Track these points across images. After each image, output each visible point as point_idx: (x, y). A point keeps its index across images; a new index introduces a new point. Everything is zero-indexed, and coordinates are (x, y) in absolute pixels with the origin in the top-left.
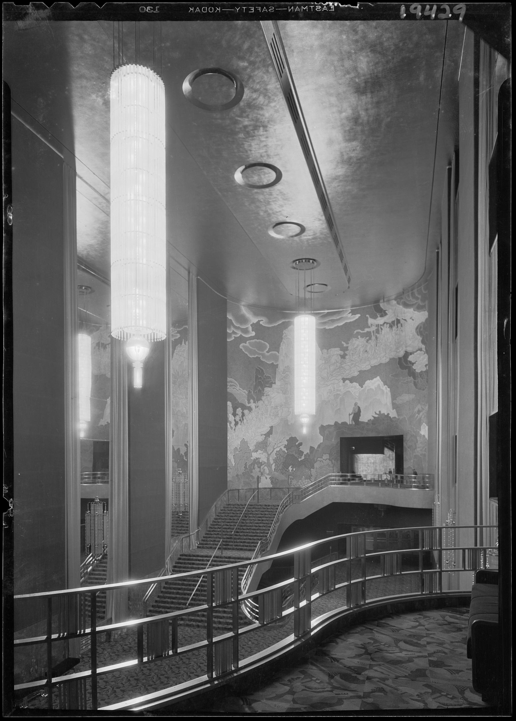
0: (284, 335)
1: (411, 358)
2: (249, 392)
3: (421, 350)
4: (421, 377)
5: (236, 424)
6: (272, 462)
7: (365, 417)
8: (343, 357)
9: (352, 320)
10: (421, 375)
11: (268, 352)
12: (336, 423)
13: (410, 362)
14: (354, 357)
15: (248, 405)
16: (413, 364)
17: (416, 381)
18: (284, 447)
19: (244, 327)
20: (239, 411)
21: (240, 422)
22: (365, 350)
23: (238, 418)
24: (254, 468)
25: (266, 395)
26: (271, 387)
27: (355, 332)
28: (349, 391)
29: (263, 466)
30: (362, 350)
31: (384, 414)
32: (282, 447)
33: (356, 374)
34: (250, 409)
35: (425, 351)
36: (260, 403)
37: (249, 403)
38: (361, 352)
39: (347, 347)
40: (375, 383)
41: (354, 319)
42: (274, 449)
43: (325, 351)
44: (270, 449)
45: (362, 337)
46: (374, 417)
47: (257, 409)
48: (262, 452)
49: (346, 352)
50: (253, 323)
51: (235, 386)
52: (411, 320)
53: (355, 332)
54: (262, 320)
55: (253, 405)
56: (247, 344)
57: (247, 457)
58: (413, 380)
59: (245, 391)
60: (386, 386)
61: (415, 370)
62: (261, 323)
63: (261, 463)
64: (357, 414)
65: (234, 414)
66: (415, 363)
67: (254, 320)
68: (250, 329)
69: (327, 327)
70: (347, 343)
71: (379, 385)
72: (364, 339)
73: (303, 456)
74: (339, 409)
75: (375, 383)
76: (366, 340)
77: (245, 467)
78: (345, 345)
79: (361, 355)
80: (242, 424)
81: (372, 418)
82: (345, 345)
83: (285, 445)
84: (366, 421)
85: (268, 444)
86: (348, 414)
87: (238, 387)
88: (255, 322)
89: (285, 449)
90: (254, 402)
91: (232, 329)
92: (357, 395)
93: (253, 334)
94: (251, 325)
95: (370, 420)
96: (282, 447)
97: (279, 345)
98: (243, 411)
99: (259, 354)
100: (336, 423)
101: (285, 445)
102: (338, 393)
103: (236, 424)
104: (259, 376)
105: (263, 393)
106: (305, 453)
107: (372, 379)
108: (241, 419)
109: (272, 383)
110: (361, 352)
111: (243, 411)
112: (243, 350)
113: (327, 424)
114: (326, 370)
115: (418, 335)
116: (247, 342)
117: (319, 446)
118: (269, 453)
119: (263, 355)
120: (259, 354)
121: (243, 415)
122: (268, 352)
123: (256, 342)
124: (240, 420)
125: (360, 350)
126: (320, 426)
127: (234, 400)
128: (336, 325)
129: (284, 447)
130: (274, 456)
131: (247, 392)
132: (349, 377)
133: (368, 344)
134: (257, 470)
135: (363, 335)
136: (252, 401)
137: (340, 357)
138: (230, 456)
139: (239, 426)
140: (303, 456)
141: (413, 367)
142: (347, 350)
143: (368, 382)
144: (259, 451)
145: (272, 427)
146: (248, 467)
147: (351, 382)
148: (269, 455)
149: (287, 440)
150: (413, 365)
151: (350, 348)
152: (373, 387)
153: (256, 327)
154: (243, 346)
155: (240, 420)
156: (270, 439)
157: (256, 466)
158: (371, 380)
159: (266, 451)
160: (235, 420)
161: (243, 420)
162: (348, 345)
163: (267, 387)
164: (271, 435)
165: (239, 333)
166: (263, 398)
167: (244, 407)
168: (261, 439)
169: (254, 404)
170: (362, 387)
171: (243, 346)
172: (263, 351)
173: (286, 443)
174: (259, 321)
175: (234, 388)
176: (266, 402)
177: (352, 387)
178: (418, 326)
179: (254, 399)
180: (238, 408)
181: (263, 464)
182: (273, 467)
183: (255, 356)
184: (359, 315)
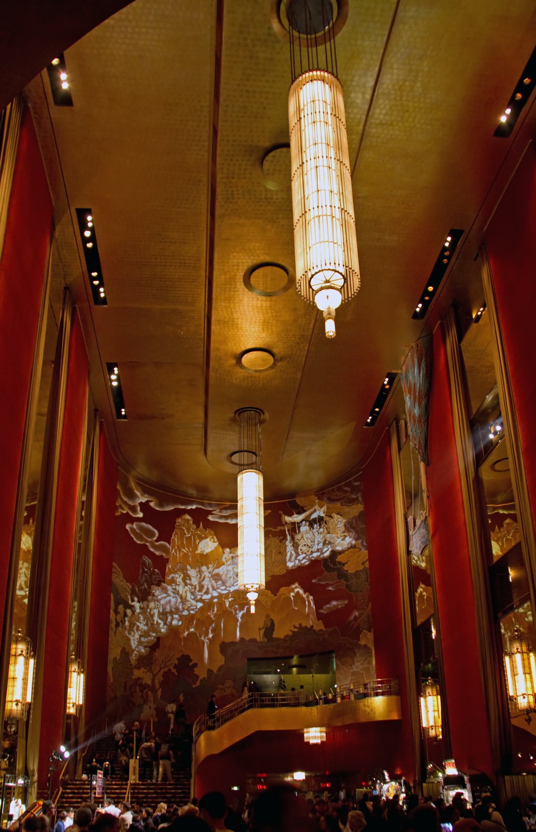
1: (339, 558)
2: (133, 587)
4: (356, 577)
6: (157, 686)
10: (356, 575)
13: (340, 563)
15: (133, 604)
16: (344, 564)
17: (350, 583)
18: (174, 667)
20: (121, 608)
21: (121, 624)
22: (278, 552)
23: (119, 619)
29: (146, 690)
30: (274, 551)
32: (171, 668)
37: (133, 601)
38: (274, 554)
42: (161, 668)
48: (145, 670)
58: (345, 582)
59: (129, 584)
60: (307, 593)
61: (347, 571)
63: (144, 685)
64: (269, 629)
66: (347, 563)
72: (276, 538)
73: (199, 681)
76: (279, 539)
77: (125, 688)
79: (273, 557)
80: (124, 627)
83: (175, 665)
85: (153, 661)
86: (258, 628)
87: (121, 578)
89: (174, 671)
90: (139, 602)
96: (171, 668)
101: (175, 665)
104: (146, 570)
105: (149, 592)
106: (201, 678)
108: (123, 620)
110: (274, 554)
113: (230, 641)
117: (219, 669)
118: (155, 673)
124: (122, 621)
125: (271, 551)
126: (220, 642)
129: (174, 667)
130: (160, 678)
131: (130, 587)
133: (282, 544)
139: (120, 628)
140: (199, 681)
141: (344, 568)
144: (142, 670)
146: (128, 688)
148: (154, 676)
149: (178, 659)
150: (344, 566)
155: (122, 621)
156: (157, 654)
157: (138, 688)
158: (287, 587)
159: (150, 670)
164: (157, 650)
169: (139, 604)
173: (176, 662)
179: (138, 597)
180: (120, 604)
182: (159, 693)
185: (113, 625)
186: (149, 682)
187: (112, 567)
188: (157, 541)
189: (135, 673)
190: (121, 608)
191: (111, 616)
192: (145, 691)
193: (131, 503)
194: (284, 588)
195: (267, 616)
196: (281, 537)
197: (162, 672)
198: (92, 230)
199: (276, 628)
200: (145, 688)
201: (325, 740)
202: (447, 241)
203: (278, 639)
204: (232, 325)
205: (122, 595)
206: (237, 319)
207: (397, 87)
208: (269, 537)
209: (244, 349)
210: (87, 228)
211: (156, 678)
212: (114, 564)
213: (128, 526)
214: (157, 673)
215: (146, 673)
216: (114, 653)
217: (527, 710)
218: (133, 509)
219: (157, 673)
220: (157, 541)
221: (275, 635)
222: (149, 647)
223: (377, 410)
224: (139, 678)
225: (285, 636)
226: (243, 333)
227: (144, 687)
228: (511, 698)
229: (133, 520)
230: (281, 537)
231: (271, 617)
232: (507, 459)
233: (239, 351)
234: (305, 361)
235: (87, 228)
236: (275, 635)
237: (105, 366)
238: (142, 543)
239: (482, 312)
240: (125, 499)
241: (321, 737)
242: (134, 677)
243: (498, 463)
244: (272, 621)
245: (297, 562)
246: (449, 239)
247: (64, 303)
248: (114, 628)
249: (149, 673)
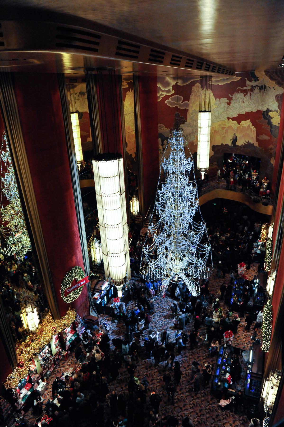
0: (192, 90)
7: (240, 143)
8: (229, 104)
9: (236, 81)
12: (222, 144)
14: (236, 105)
19: (167, 89)
26: (184, 123)
27: (237, 88)
28: (231, 126)
30: (241, 101)
31: (251, 143)
33: (236, 115)
39: (232, 98)
40: (247, 123)
41: (238, 80)
43: (218, 99)
45: (242, 92)
46: (245, 144)
49: (231, 101)
50: (173, 85)
51: (162, 128)
53: (237, 88)
54: (179, 82)
56: (170, 100)
62: (178, 84)
64: (235, 140)
67: (173, 83)
68: (172, 89)
69: (220, 84)
70: (232, 95)
71: (249, 125)
74: (225, 136)
75: (247, 123)
78: (231, 96)
81: (244, 144)
82: (231, 96)
84: (240, 145)
88: (174, 84)
91: (161, 92)
92: (236, 128)
93: (173, 92)
94: (172, 87)
95: (242, 145)
97: (189, 97)
99: (177, 104)
100: (222, 144)
102: (225, 126)
107: (246, 120)
112: (167, 104)
114: (218, 112)
116: (170, 98)
119: (180, 105)
120: (177, 104)
123: (175, 97)
128: (225, 83)
131: (170, 130)
132: (232, 117)
135: (242, 91)
137: (227, 104)
142: (232, 100)
143: (243, 122)
147: (233, 120)
151: (233, 99)
152: (246, 126)
153: (175, 87)
154: (167, 102)
162: (232, 97)
163: (181, 124)
165: (165, 94)
170: (239, 124)
171: (167, 102)
174: (177, 83)
177: (233, 124)
183: (174, 106)
184: (241, 77)
188: (182, 102)
194: (243, 121)
195: (234, 134)
196: (245, 94)
199: (237, 140)
203: (238, 146)
208: (239, 93)
220: (182, 102)
221: (237, 144)
225: (241, 145)
230: (245, 94)
231: (236, 135)
236: (237, 144)
244: (236, 137)
245: (251, 108)
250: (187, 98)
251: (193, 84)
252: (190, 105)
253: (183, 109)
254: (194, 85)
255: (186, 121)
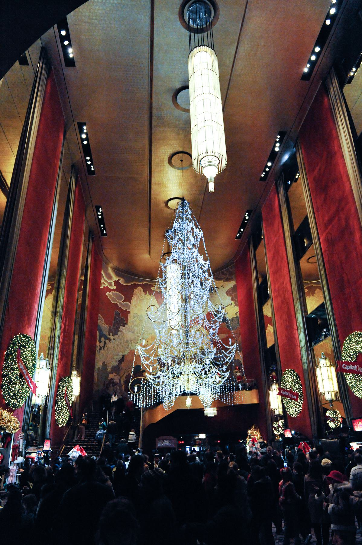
2: (110, 327)
3: (231, 304)
5: (100, 349)
6: (122, 383)
11: (123, 302)
15: (109, 337)
20: (103, 339)
21: (103, 348)
23: (102, 345)
24: (110, 387)
25: (121, 332)
26: (124, 326)
29: (116, 386)
34: (110, 340)
35: (234, 304)
36: (116, 337)
37: (109, 335)
42: (125, 373)
44: (121, 373)
47: (114, 340)
48: (116, 374)
52: (222, 287)
55: (111, 337)
57: (106, 377)
59: (107, 325)
63: (115, 383)
65: (100, 342)
77: (104, 385)
87: (103, 322)
90: (113, 335)
98: (105, 340)
103: (100, 349)
109: (125, 324)
111: (105, 340)
115: (228, 295)
119: (120, 303)
121: (105, 343)
122: (123, 302)
124: (103, 347)
127: (100, 331)
131: (108, 327)
134: (112, 388)
136: (111, 334)
138: (95, 374)
139: (102, 351)
144: (114, 374)
145: (123, 356)
148: (121, 377)
155: (103, 347)
156: (122, 365)
159: (118, 374)
160: (100, 346)
161: (105, 347)
163: (121, 326)
166: (119, 333)
167: (106, 338)
168: (115, 364)
172: (120, 300)
175: (101, 322)
176: (121, 337)
178: (228, 290)
181: (116, 385)
185: (98, 348)
186: (118, 381)
187: (98, 317)
189: (110, 376)
190: (103, 339)
191: (97, 344)
192: (115, 387)
193: (109, 281)
197: (125, 375)
198: (86, 134)
200: (115, 385)
201: (216, 414)
202: (277, 138)
204: (163, 185)
205: (104, 332)
206: (165, 182)
207: (247, 54)
209: (169, 198)
210: (83, 133)
211: (122, 378)
212: (99, 315)
213: (107, 293)
214: (122, 376)
215: (116, 376)
216: (99, 364)
217: (330, 400)
218: (110, 284)
219: (122, 376)
222: (118, 361)
223: (242, 230)
224: (112, 379)
226: (168, 190)
227: (115, 384)
228: (321, 393)
229: (110, 290)
232: (315, 256)
233: (167, 199)
234: (202, 204)
235: (83, 133)
237: (94, 208)
238: (115, 303)
239: (298, 176)
240: (106, 279)
241: (214, 413)
242: (109, 378)
243: (310, 259)
246: (279, 137)
247: (71, 174)
248: (99, 351)
249: (117, 376)
250: (128, 299)
251: (136, 286)
252: (132, 307)
253: (124, 309)
254: (136, 288)
255: (127, 324)
